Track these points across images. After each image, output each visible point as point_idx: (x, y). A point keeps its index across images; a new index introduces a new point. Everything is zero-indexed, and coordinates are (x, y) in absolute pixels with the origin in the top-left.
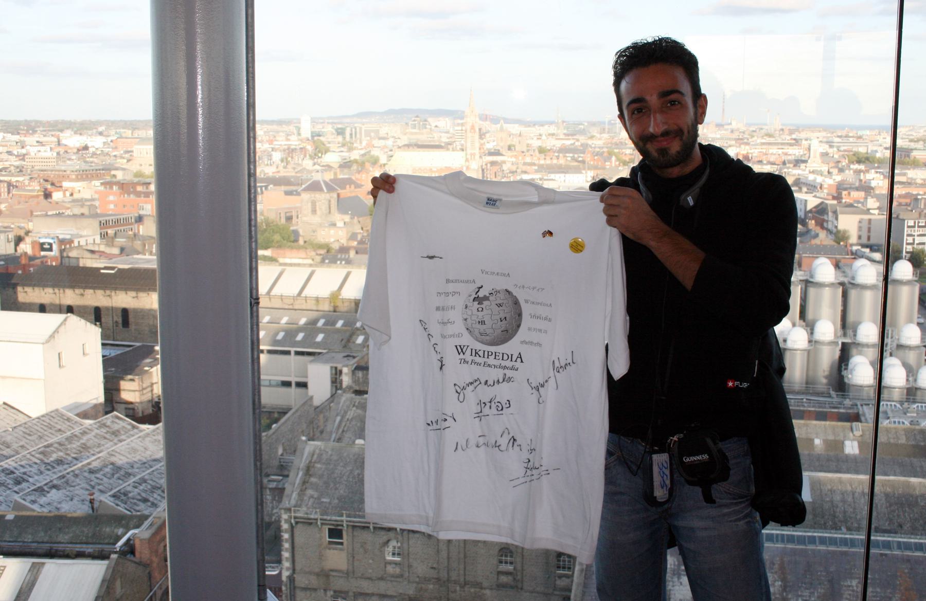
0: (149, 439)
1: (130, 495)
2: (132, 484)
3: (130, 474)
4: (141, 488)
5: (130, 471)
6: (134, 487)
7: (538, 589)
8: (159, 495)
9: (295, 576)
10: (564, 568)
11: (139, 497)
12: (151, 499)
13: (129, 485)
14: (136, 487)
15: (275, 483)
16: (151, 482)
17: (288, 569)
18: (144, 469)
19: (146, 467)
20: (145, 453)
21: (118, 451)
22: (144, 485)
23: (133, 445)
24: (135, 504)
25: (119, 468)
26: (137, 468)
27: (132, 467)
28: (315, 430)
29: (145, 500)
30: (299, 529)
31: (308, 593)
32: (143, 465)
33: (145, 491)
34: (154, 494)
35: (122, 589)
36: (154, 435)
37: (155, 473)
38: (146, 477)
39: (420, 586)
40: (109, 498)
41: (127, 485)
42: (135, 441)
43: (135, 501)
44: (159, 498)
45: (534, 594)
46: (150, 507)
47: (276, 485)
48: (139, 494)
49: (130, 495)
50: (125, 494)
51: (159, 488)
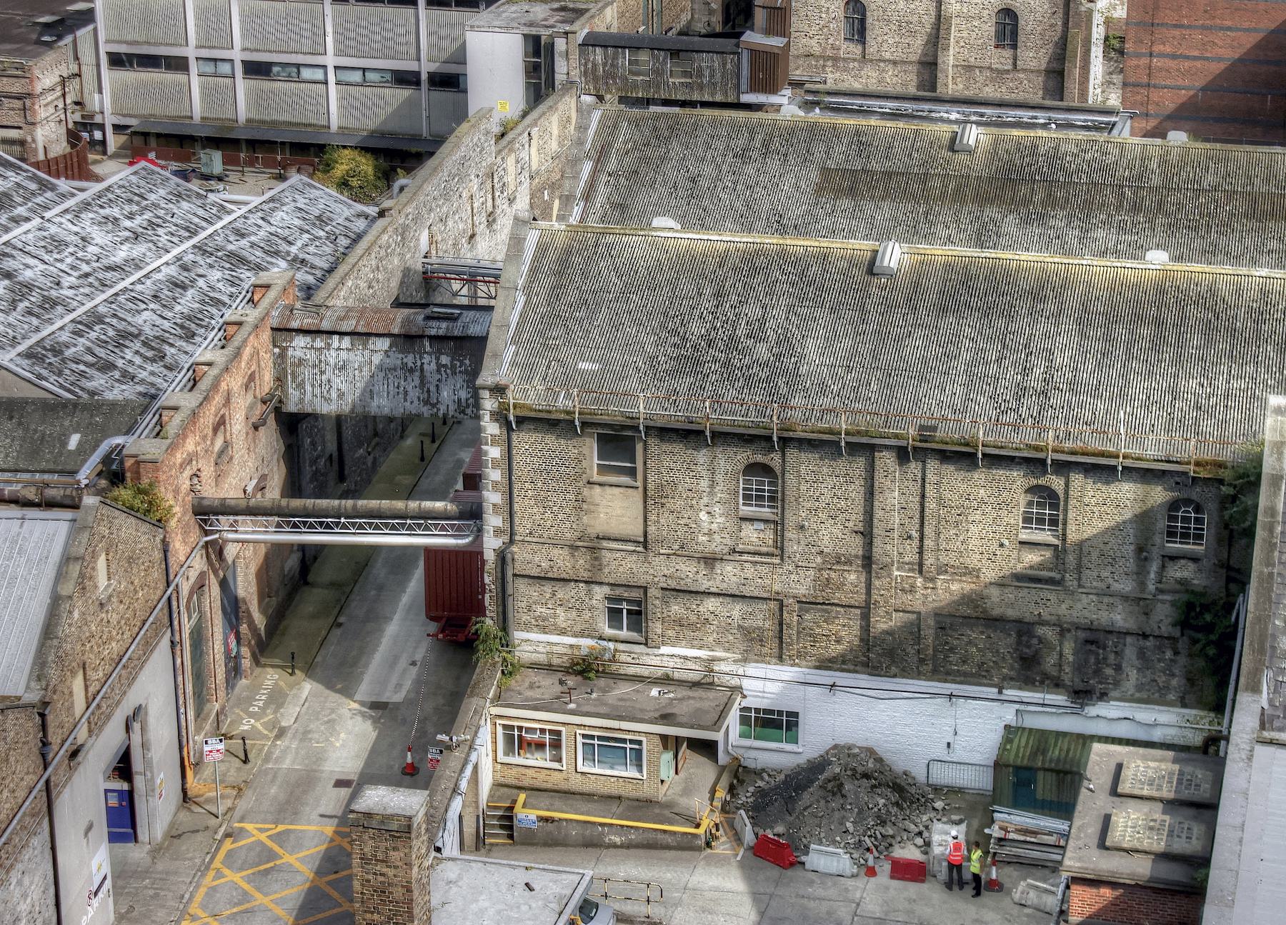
0: (91, 215)
1: (69, 353)
2: (71, 327)
3: (54, 303)
4: (93, 335)
5: (54, 293)
6: (74, 333)
7: (1116, 587)
8: (137, 352)
9: (515, 549)
10: (1185, 536)
11: (90, 359)
12: (120, 363)
13: (61, 328)
14: (78, 334)
15: (444, 325)
16: (114, 322)
17: (498, 532)
18: (87, 290)
19: (91, 285)
20: (83, 249)
21: (20, 245)
22: (97, 328)
23: (53, 229)
24: (82, 374)
25: (29, 287)
26: (71, 288)
27: (58, 284)
28: (497, 194)
29: (106, 367)
30: (525, 441)
31: (548, 588)
32: (81, 281)
33: (102, 343)
34: (127, 351)
35: (109, 579)
36: (101, 207)
37: (121, 299)
38: (102, 309)
39: (825, 574)
40: (19, 360)
41: (58, 325)
42: (58, 220)
43: (82, 367)
44: (138, 360)
45: (1106, 600)
46: (118, 381)
47: (447, 328)
48: (89, 351)
49: (69, 353)
50: (57, 350)
51: (136, 336)
